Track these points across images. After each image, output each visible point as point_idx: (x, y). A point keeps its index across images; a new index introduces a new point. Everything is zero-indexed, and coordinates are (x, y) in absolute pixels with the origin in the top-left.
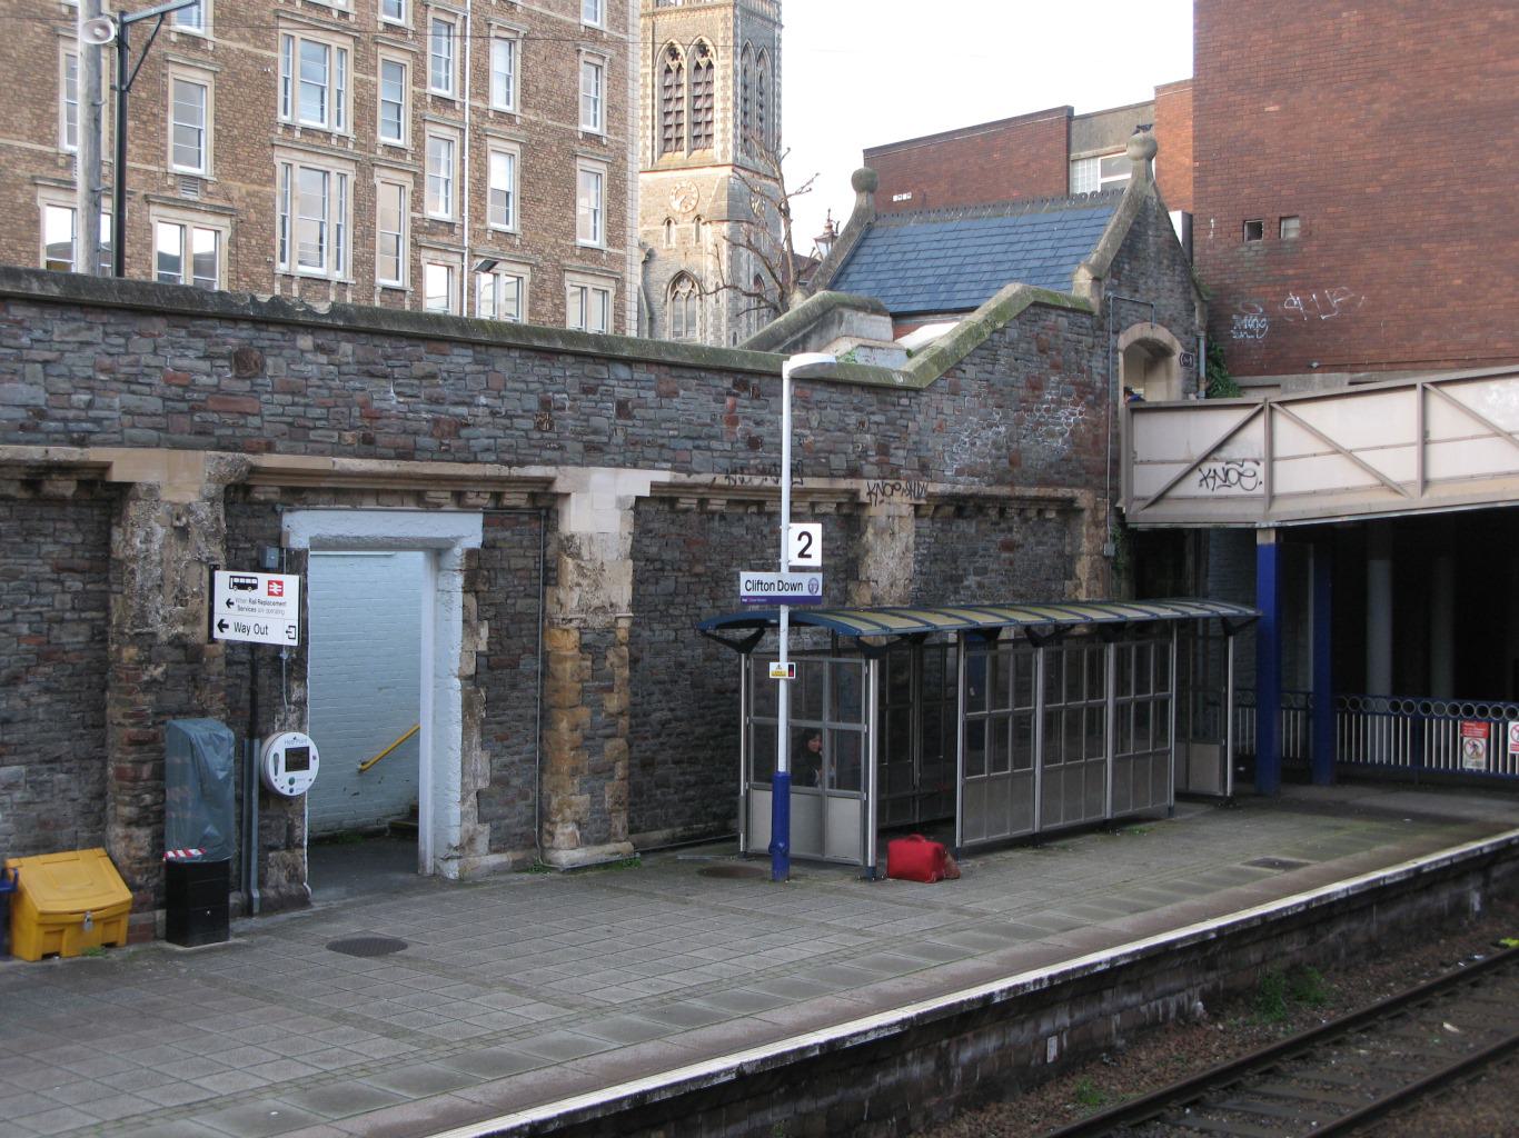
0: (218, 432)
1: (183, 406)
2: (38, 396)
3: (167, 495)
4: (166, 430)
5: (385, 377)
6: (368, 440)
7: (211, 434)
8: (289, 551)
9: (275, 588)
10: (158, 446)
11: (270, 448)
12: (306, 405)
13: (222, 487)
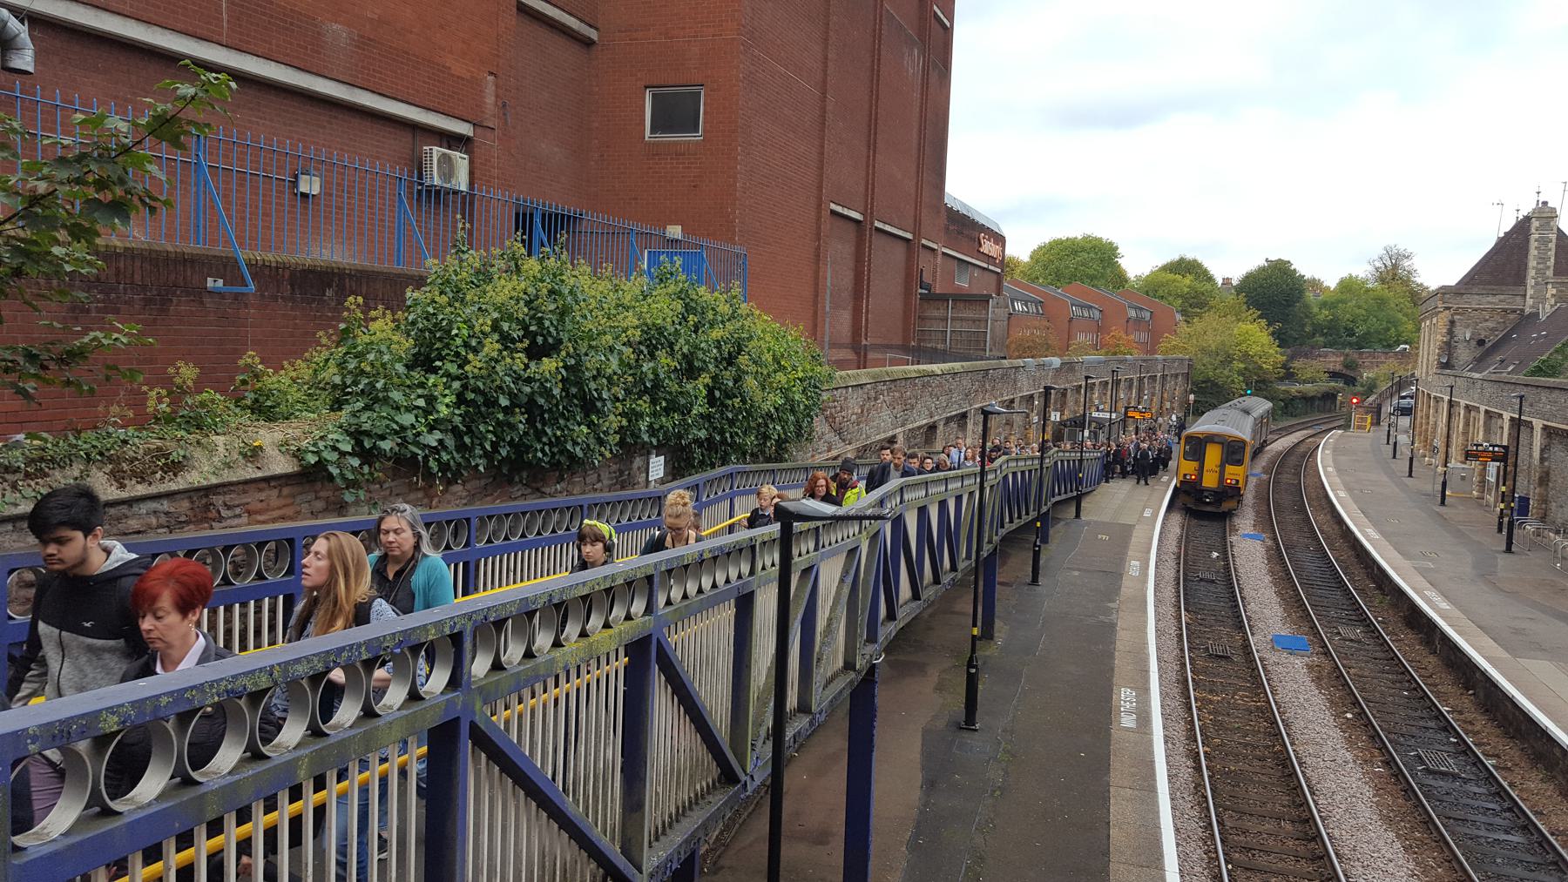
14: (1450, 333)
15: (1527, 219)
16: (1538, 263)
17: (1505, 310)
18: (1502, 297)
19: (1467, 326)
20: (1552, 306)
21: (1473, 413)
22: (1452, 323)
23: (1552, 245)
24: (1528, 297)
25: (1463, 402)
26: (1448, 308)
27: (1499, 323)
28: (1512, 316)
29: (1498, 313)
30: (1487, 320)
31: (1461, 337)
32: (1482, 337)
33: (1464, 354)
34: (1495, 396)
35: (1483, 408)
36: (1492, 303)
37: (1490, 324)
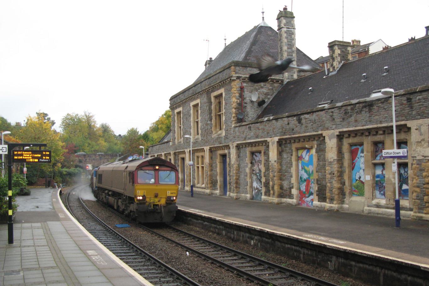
14: (241, 96)
16: (288, 48)
20: (340, 63)
22: (242, 89)
27: (269, 89)
28: (276, 85)
30: (262, 88)
31: (247, 100)
33: (251, 113)
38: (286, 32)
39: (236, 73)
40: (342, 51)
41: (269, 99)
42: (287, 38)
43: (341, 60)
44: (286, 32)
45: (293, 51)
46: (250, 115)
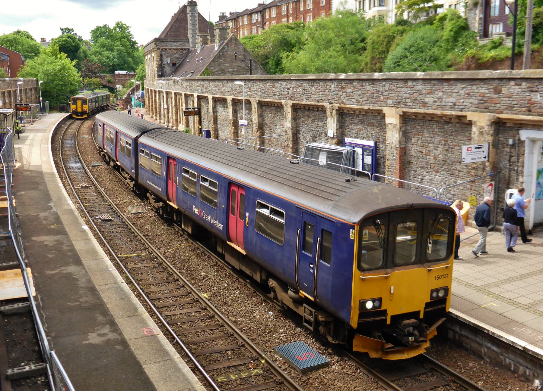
0: (490, 108)
1: (482, 102)
2: (454, 100)
3: (479, 124)
4: (478, 108)
5: (536, 91)
6: (530, 111)
7: (488, 109)
8: (519, 140)
9: (469, 149)
10: (476, 111)
11: (502, 113)
12: (512, 101)
13: (490, 122)
14: (161, 60)
15: (185, 7)
17: (182, 49)
18: (180, 43)
19: (168, 57)
21: (178, 97)
22: (161, 55)
23: (197, 19)
24: (190, 43)
25: (173, 92)
26: (158, 49)
27: (180, 55)
28: (185, 52)
29: (179, 51)
30: (175, 54)
31: (165, 62)
32: (174, 62)
33: (167, 70)
34: (188, 87)
35: (183, 93)
36: (176, 46)
37: (177, 56)
38: (190, 16)
39: (157, 46)
40: (203, 39)
41: (180, 61)
42: (191, 20)
43: (203, 44)
44: (190, 16)
45: (196, 29)
46: (167, 72)
